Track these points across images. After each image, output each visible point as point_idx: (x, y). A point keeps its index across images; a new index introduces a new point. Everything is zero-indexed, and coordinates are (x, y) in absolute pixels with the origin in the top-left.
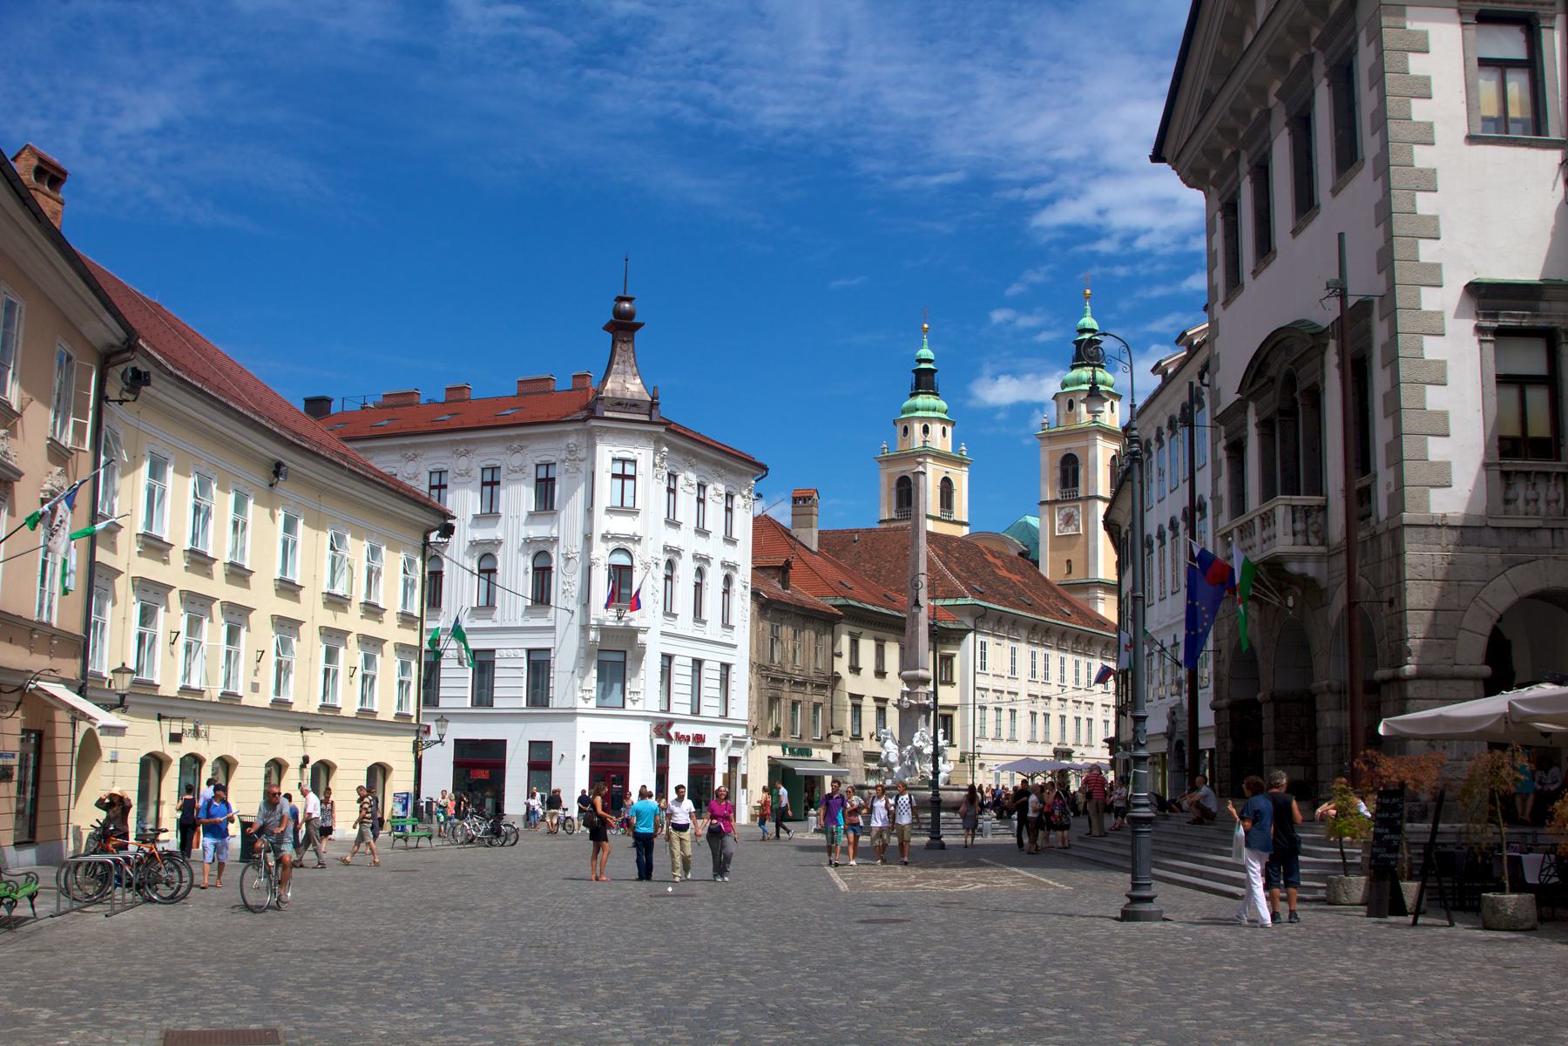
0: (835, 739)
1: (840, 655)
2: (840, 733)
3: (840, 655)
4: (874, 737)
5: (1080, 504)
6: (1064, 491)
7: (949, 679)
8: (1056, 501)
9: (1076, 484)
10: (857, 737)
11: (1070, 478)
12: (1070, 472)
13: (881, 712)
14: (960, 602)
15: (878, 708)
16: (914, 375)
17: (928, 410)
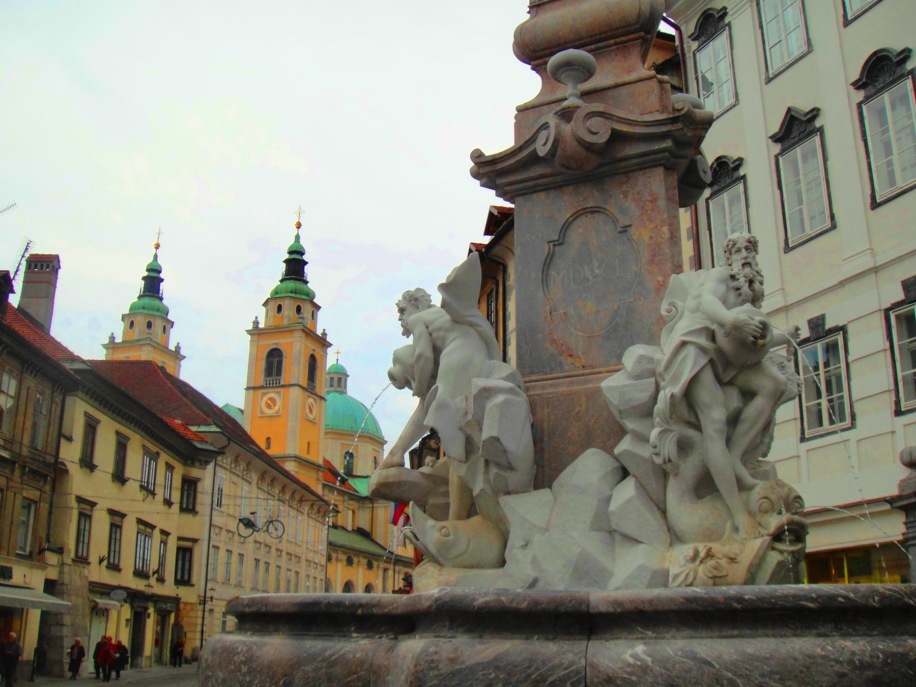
0: (52, 558)
1: (70, 439)
2: (60, 551)
3: (70, 439)
4: (105, 563)
5: (281, 390)
6: (268, 379)
7: (191, 507)
8: (262, 387)
9: (279, 373)
10: (82, 560)
11: (275, 369)
12: (275, 364)
13: (115, 528)
14: (203, 429)
15: (112, 525)
16: (143, 282)
17: (153, 310)
